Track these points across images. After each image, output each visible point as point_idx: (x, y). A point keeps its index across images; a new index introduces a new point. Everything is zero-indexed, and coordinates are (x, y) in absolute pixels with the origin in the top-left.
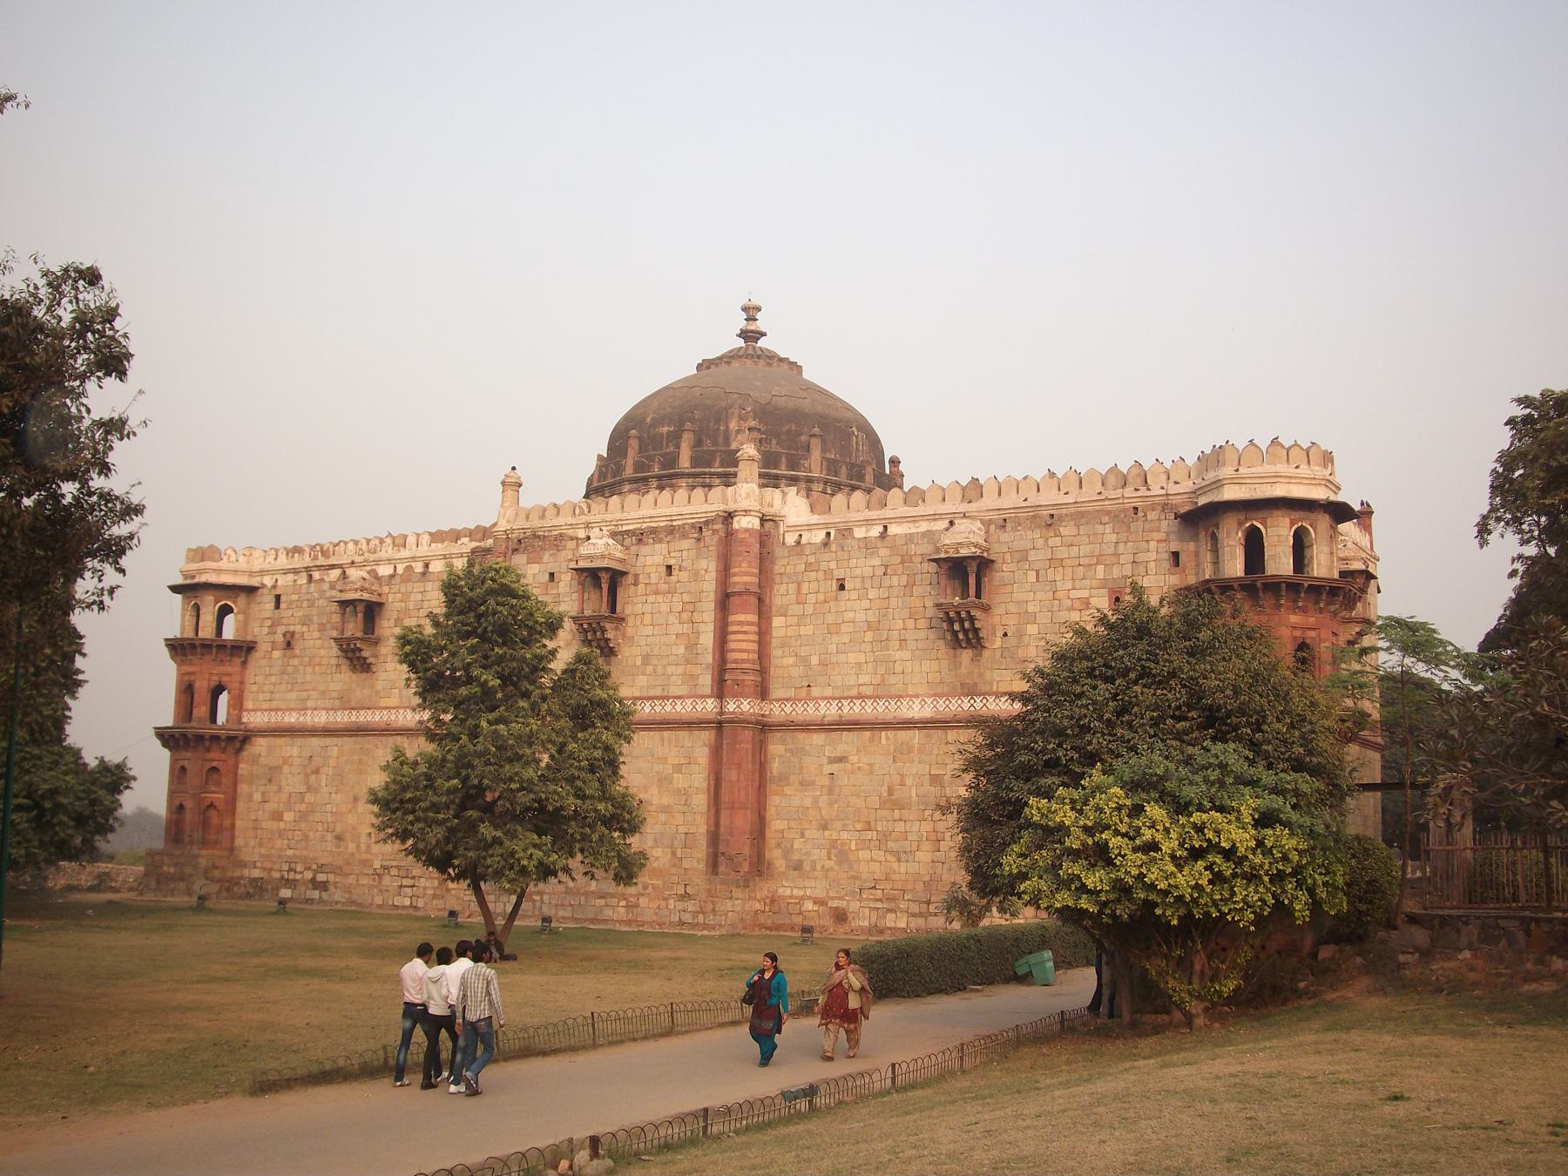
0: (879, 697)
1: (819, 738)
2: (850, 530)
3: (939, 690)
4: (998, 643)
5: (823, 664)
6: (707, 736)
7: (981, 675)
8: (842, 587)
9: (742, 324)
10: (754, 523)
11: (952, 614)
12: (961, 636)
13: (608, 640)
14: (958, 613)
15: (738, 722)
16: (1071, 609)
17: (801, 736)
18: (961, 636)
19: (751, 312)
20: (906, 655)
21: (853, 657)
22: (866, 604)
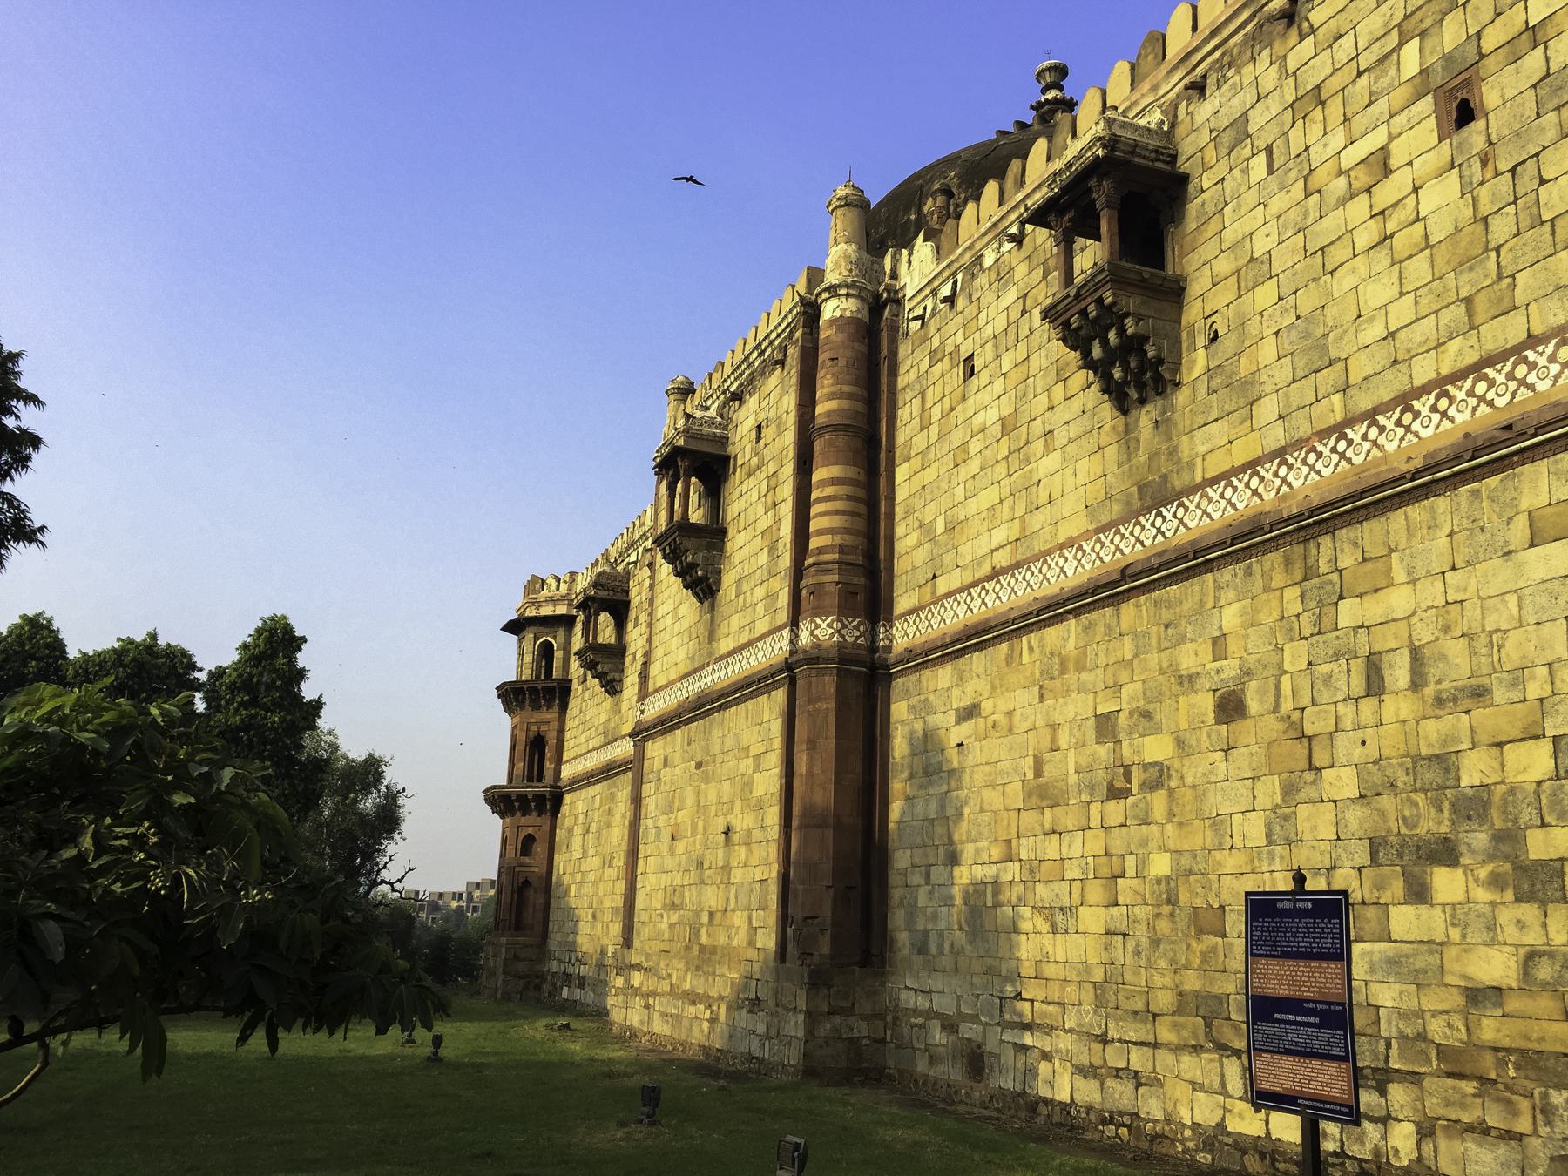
0: (1018, 565)
1: (943, 675)
3: (1105, 519)
4: (1197, 362)
5: (950, 529)
6: (780, 695)
7: (1173, 452)
11: (1075, 322)
14: (1084, 313)
15: (814, 657)
16: (1342, 202)
17: (927, 674)
20: (1052, 461)
21: (989, 497)
22: (999, 385)
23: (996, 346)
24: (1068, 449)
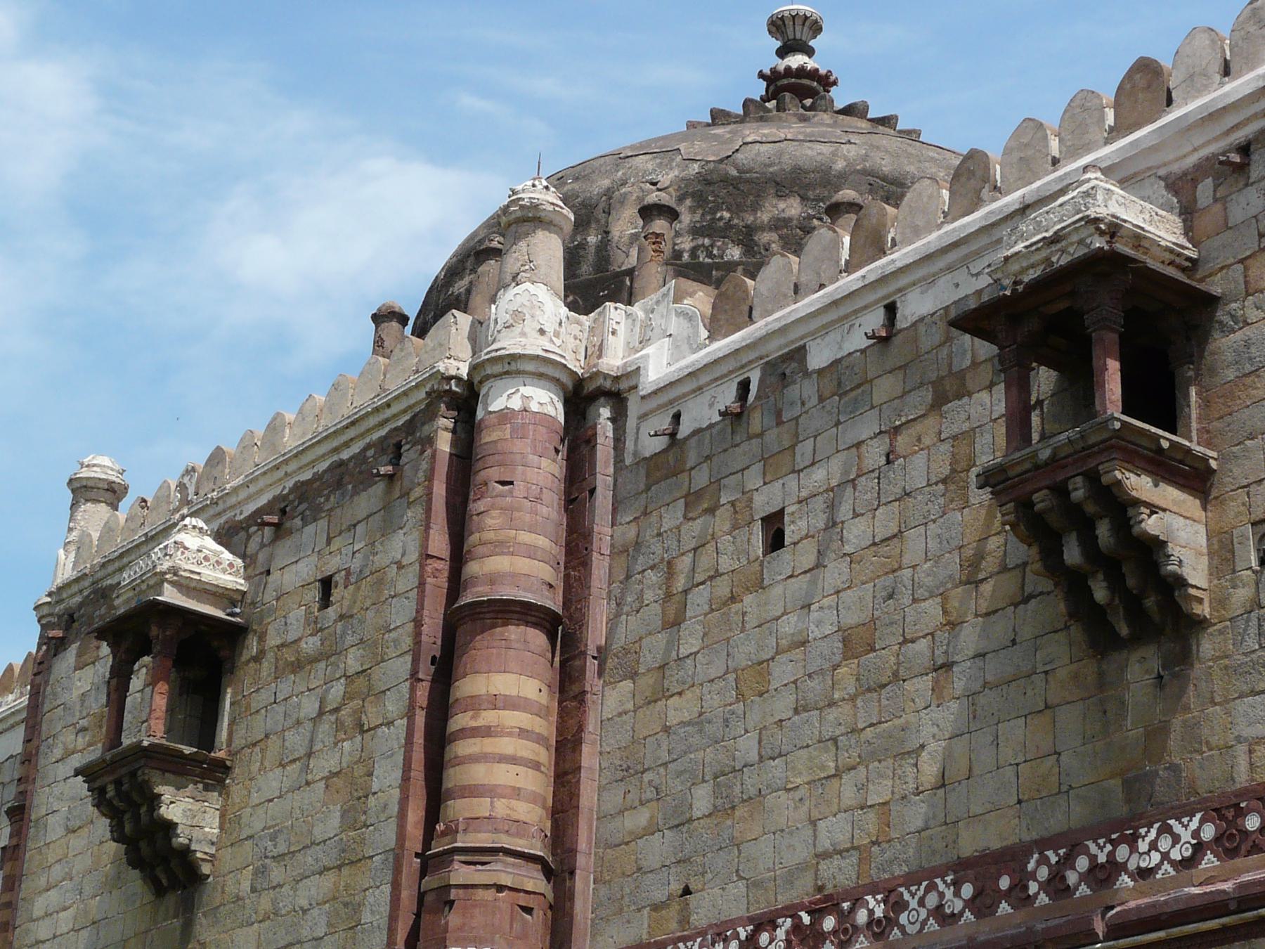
2: (798, 354)
5: (724, 809)
8: (776, 541)
9: (771, 62)
10: (544, 401)
11: (1042, 500)
12: (1100, 593)
13: (170, 826)
14: (1061, 491)
18: (1100, 593)
19: (792, 33)
22: (836, 573)
23: (832, 507)
24: (981, 700)
